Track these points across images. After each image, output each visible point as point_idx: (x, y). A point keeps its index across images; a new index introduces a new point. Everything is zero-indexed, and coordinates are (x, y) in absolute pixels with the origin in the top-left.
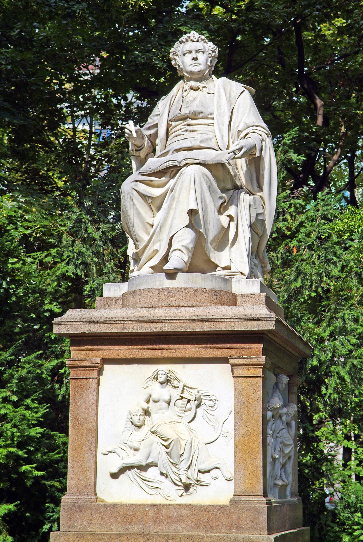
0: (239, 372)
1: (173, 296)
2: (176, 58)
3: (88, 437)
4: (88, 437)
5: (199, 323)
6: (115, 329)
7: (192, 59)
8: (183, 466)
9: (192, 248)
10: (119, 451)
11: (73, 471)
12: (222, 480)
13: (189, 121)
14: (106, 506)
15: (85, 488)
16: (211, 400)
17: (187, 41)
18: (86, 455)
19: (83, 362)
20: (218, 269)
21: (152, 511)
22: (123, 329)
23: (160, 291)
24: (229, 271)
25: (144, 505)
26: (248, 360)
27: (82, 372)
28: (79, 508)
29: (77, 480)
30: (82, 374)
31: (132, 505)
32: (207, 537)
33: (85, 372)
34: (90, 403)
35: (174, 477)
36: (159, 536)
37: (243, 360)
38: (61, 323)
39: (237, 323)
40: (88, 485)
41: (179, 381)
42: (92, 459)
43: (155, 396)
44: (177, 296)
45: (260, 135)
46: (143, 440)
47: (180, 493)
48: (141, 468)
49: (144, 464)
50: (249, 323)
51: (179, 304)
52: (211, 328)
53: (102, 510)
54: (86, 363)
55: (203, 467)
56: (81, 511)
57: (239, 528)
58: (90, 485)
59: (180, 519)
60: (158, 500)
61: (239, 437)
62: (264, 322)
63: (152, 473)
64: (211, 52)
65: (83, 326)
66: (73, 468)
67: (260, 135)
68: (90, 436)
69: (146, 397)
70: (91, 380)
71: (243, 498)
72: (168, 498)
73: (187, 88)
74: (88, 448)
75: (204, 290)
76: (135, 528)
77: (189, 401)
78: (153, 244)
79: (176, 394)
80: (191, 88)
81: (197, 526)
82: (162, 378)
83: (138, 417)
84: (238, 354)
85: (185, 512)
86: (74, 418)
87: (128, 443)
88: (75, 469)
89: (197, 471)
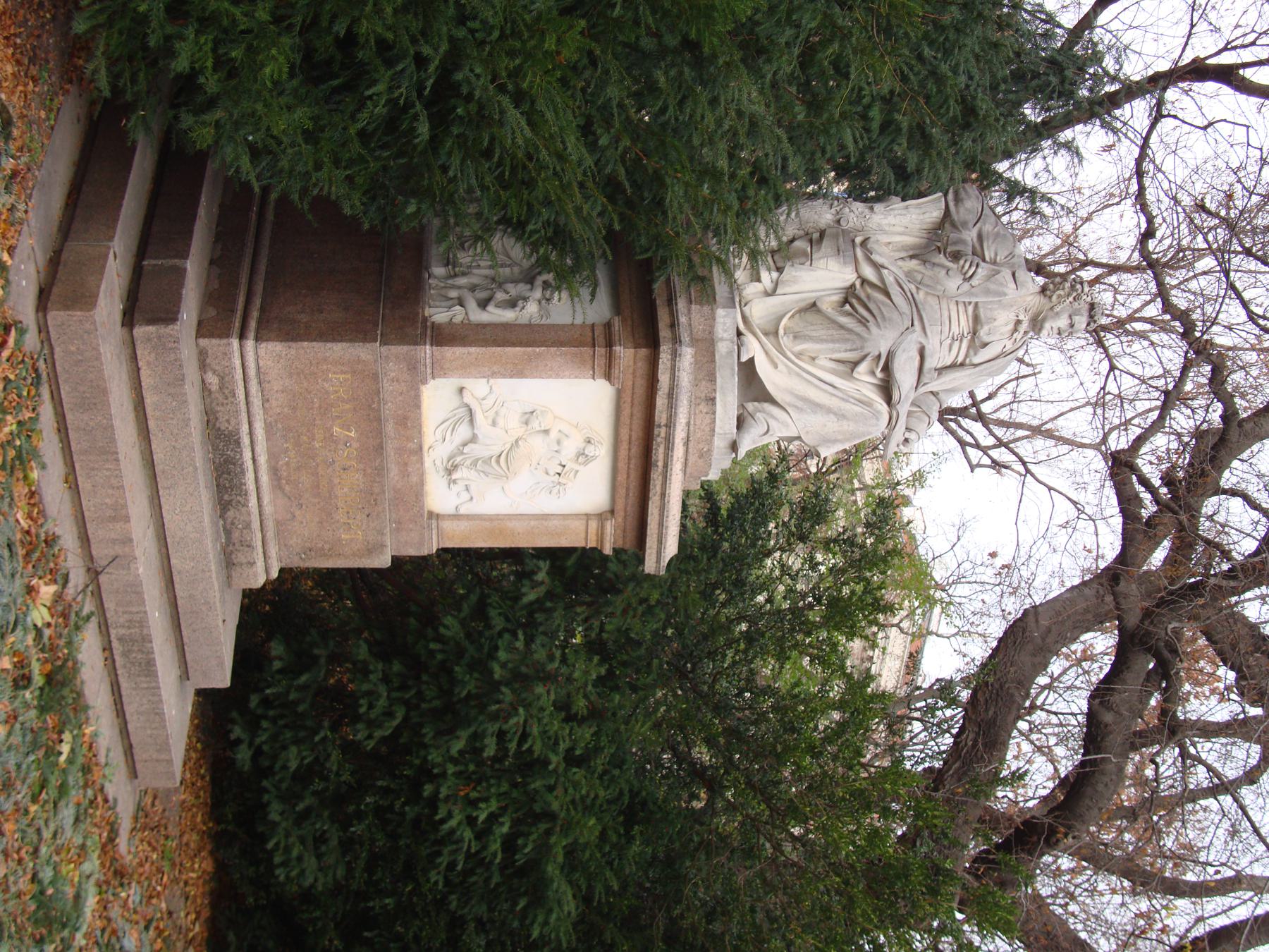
0: (593, 525)
1: (701, 456)
2: (1071, 299)
6: (661, 416)
12: (458, 502)
14: (417, 397)
21: (411, 446)
30: (600, 361)
35: (459, 459)
41: (585, 463)
43: (565, 443)
47: (438, 463)
48: (472, 421)
50: (654, 551)
53: (412, 393)
54: (615, 372)
59: (405, 474)
61: (510, 524)
65: (667, 380)
71: (434, 532)
73: (1021, 317)
76: (390, 428)
78: (786, 366)
80: (1018, 322)
82: (590, 450)
85: (414, 479)
86: (539, 354)
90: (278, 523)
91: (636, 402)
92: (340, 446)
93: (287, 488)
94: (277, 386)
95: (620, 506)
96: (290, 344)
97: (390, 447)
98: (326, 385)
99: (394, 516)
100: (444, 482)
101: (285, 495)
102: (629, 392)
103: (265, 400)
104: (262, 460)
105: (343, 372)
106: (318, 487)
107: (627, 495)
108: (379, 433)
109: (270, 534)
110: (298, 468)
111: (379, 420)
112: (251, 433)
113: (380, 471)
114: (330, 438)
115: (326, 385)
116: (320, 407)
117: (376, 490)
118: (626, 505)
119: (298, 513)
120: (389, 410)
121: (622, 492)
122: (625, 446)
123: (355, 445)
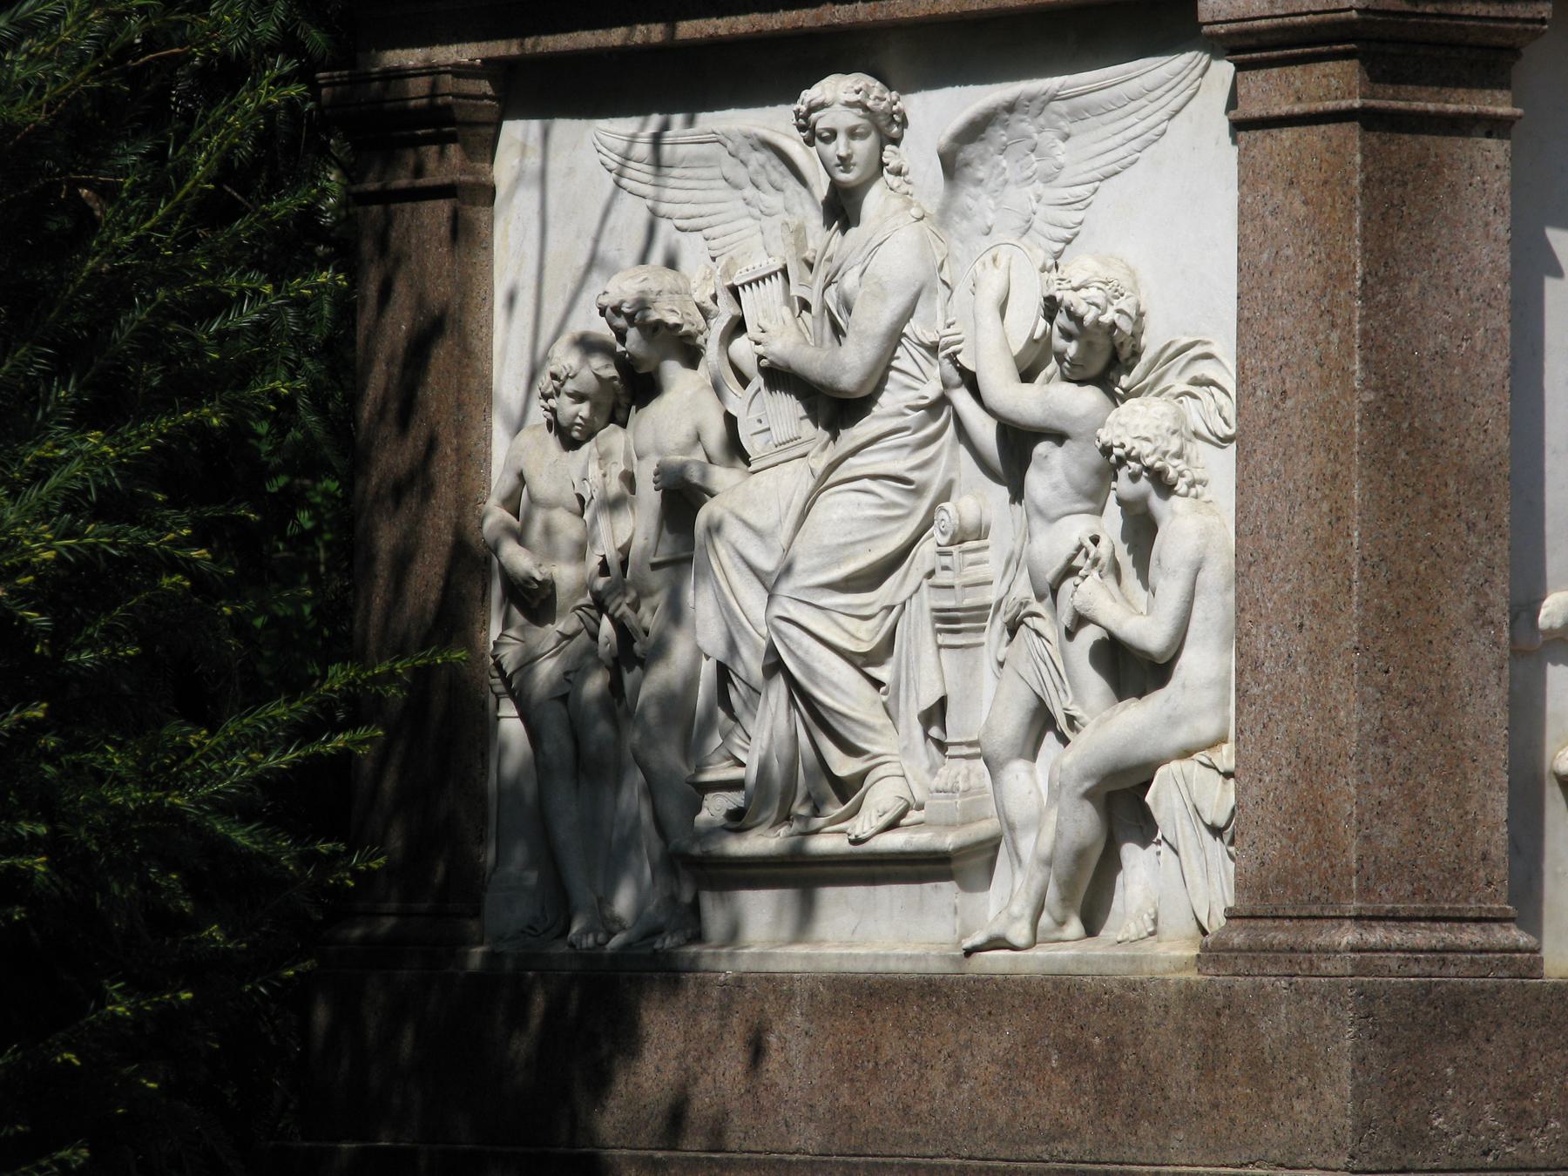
3: (1471, 526)
4: (1471, 526)
11: (1387, 760)
18: (1459, 654)
29: (1407, 821)
34: (1478, 289)
40: (1477, 855)
42: (1493, 680)
56: (1464, 1035)
58: (1485, 857)
66: (1384, 740)
68: (1482, 525)
74: (1468, 604)
88: (1400, 748)
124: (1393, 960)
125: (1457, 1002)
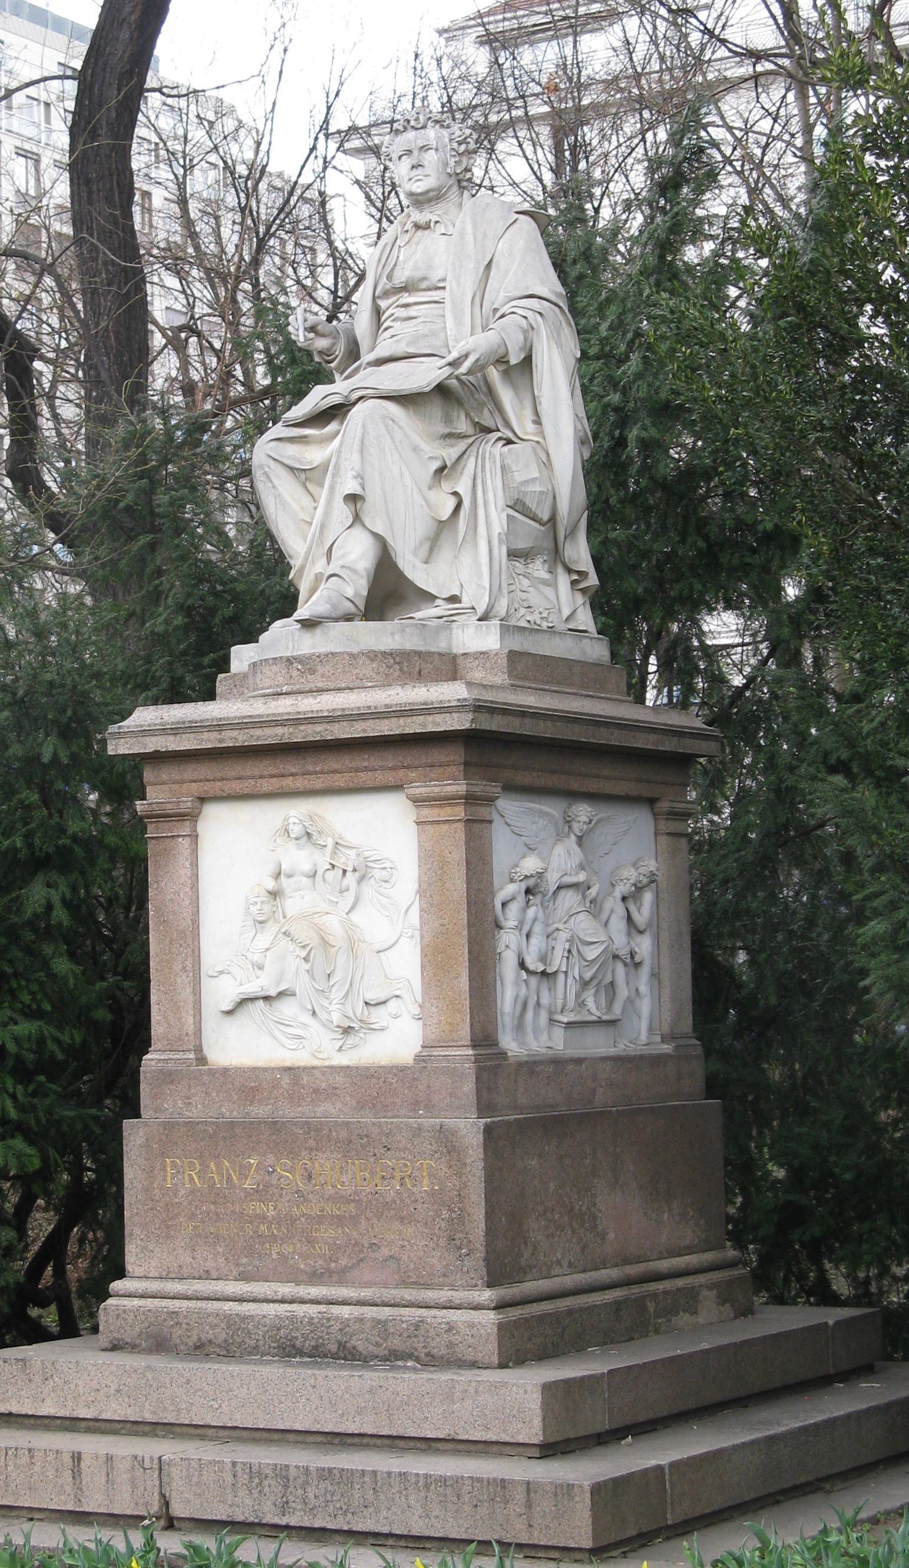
1: (312, 671)
5: (345, 724)
6: (208, 741)
7: (413, 167)
8: (336, 995)
9: (366, 569)
10: (235, 970)
13: (407, 298)
15: (180, 1039)
16: (384, 868)
17: (405, 129)
18: (179, 980)
19: (164, 806)
20: (438, 602)
21: (286, 1081)
22: (221, 741)
23: (290, 661)
24: (457, 605)
25: (273, 1069)
26: (437, 789)
27: (166, 825)
28: (168, 1077)
29: (166, 1025)
31: (254, 1069)
32: (374, 1124)
33: (171, 824)
36: (295, 1124)
37: (428, 789)
38: (119, 735)
39: (409, 720)
44: (320, 670)
45: (525, 317)
46: (268, 949)
49: (273, 993)
50: (430, 718)
51: (320, 685)
52: (364, 731)
54: (170, 809)
55: (372, 996)
56: (172, 1082)
57: (429, 1107)
59: (331, 1093)
60: (301, 1058)
62: (455, 715)
63: (287, 1009)
64: (455, 145)
65: (154, 739)
67: (525, 317)
69: (271, 868)
70: (180, 839)
72: (317, 1054)
75: (373, 656)
76: (260, 1111)
77: (345, 871)
79: (323, 860)
80: (417, 226)
81: (361, 1105)
82: (296, 830)
83: (258, 906)
84: (422, 779)
85: (339, 1080)
86: (157, 911)
87: (249, 955)
89: (361, 1004)
90: (405, 1284)
91: (219, 775)
92: (274, 1182)
93: (343, 1262)
94: (186, 1258)
95: (390, 778)
96: (126, 1232)
97: (288, 1112)
98: (182, 1192)
99: (403, 1112)
100: (374, 1039)
101: (353, 1267)
102: (207, 786)
103: (207, 1276)
104: (286, 1289)
105: (164, 1168)
106: (339, 1218)
107: (366, 769)
108: (252, 1127)
109: (408, 1294)
110: (311, 1241)
111: (232, 1125)
112: (241, 1300)
113: (312, 1129)
114: (261, 1193)
115: (182, 1192)
116: (215, 1203)
117: (344, 1134)
118: (383, 768)
119: (385, 1252)
120: (230, 1111)
121: (364, 778)
122: (289, 783)
123: (270, 1159)
124: (153, 1063)
125: (170, 1073)
